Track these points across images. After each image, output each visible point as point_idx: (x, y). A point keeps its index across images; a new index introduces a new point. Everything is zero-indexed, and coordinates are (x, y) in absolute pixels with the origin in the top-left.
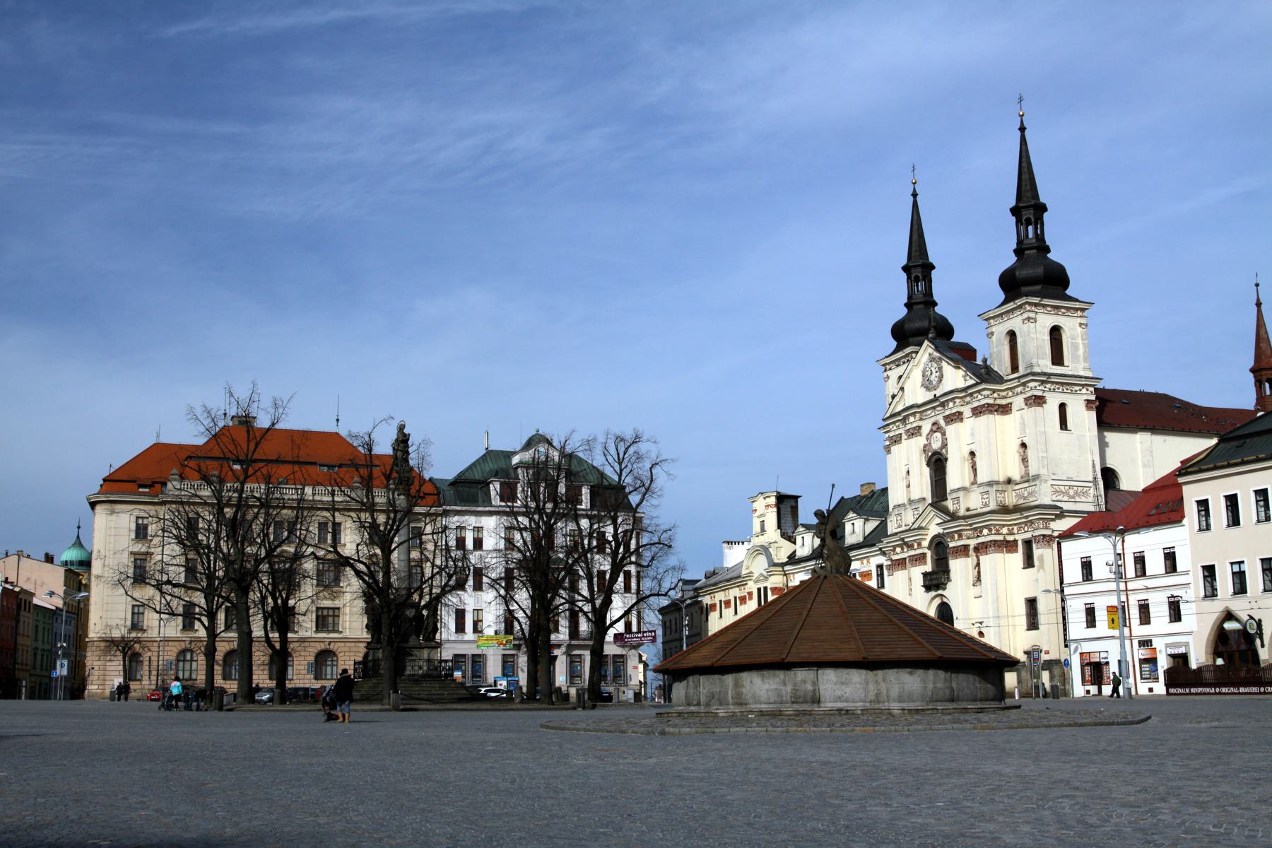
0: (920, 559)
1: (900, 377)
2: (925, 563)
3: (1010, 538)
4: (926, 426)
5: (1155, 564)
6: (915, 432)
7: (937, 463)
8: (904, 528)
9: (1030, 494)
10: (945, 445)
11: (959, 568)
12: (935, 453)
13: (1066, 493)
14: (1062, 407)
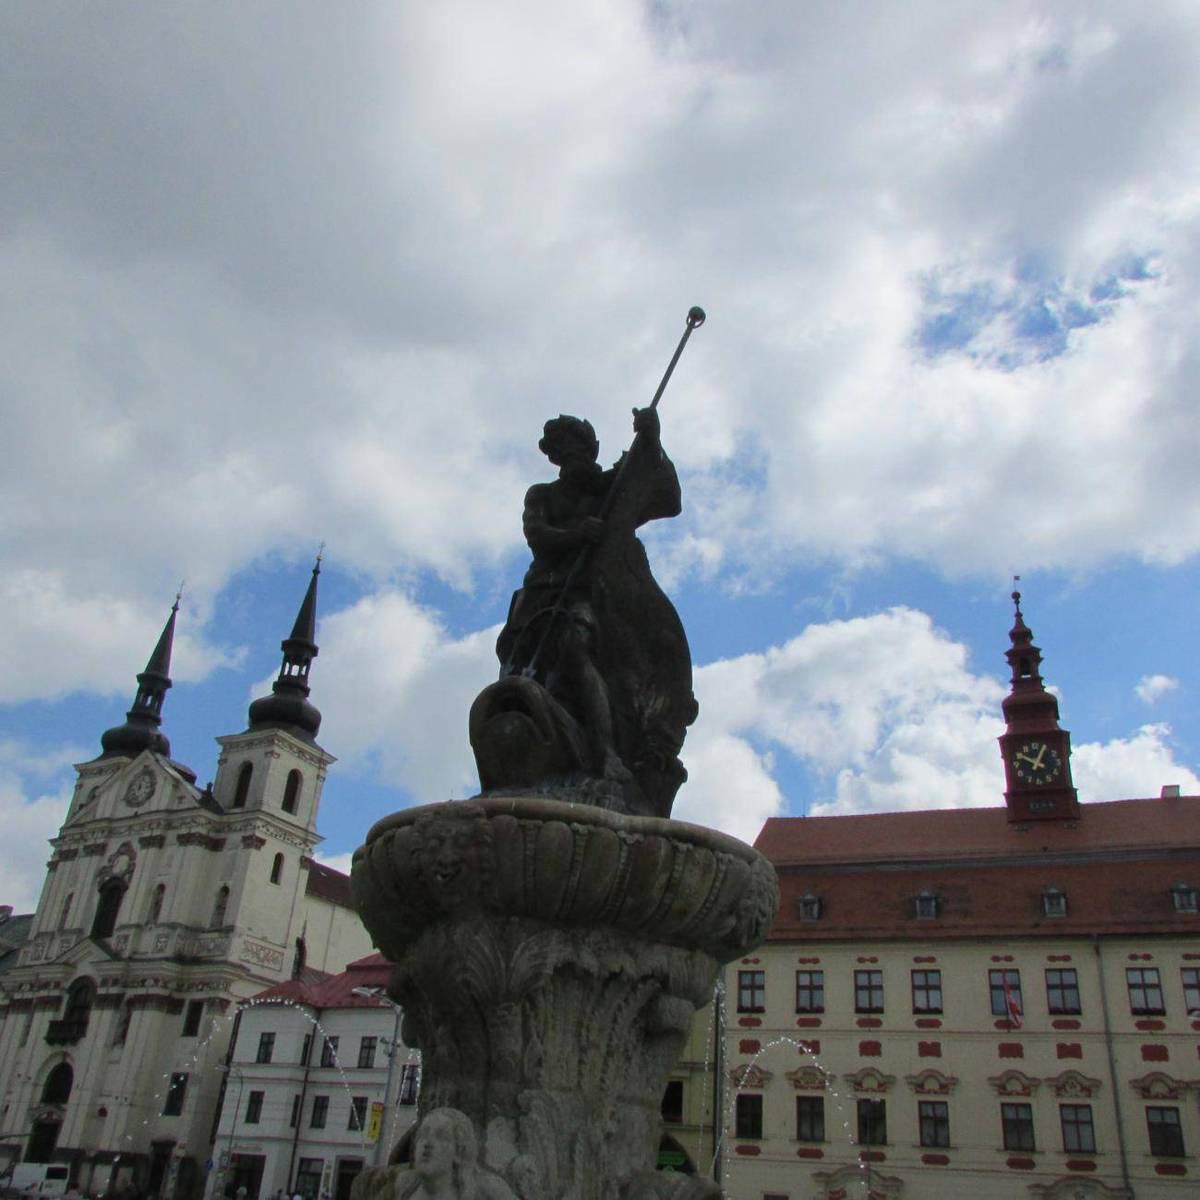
0: (52, 1003)
1: (96, 788)
2: (57, 1009)
3: (176, 996)
4: (114, 846)
5: (347, 1054)
6: (100, 849)
7: (112, 891)
8: (43, 961)
9: (217, 947)
10: (130, 870)
11: (101, 1021)
12: (115, 878)
13: (256, 954)
14: (279, 858)
